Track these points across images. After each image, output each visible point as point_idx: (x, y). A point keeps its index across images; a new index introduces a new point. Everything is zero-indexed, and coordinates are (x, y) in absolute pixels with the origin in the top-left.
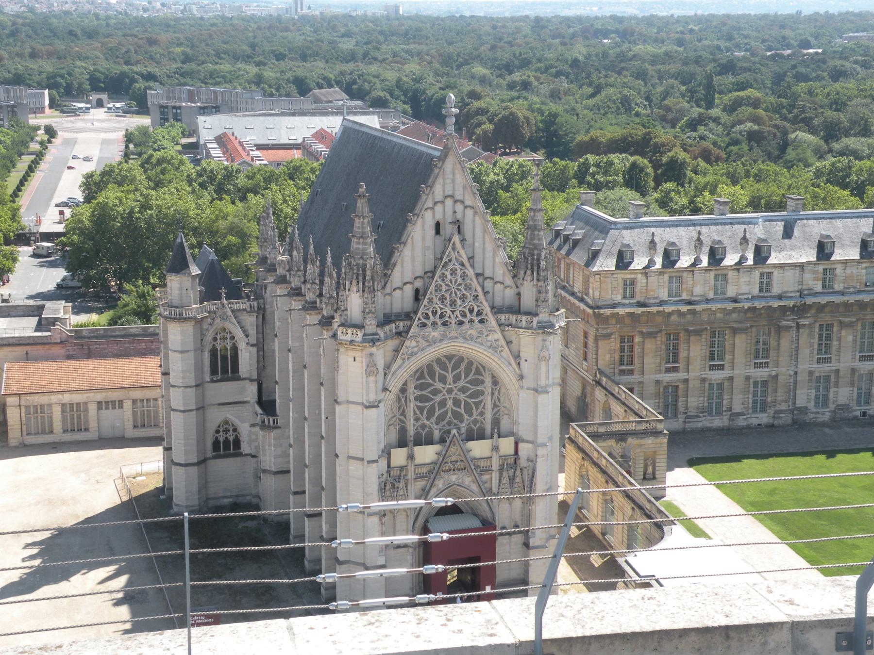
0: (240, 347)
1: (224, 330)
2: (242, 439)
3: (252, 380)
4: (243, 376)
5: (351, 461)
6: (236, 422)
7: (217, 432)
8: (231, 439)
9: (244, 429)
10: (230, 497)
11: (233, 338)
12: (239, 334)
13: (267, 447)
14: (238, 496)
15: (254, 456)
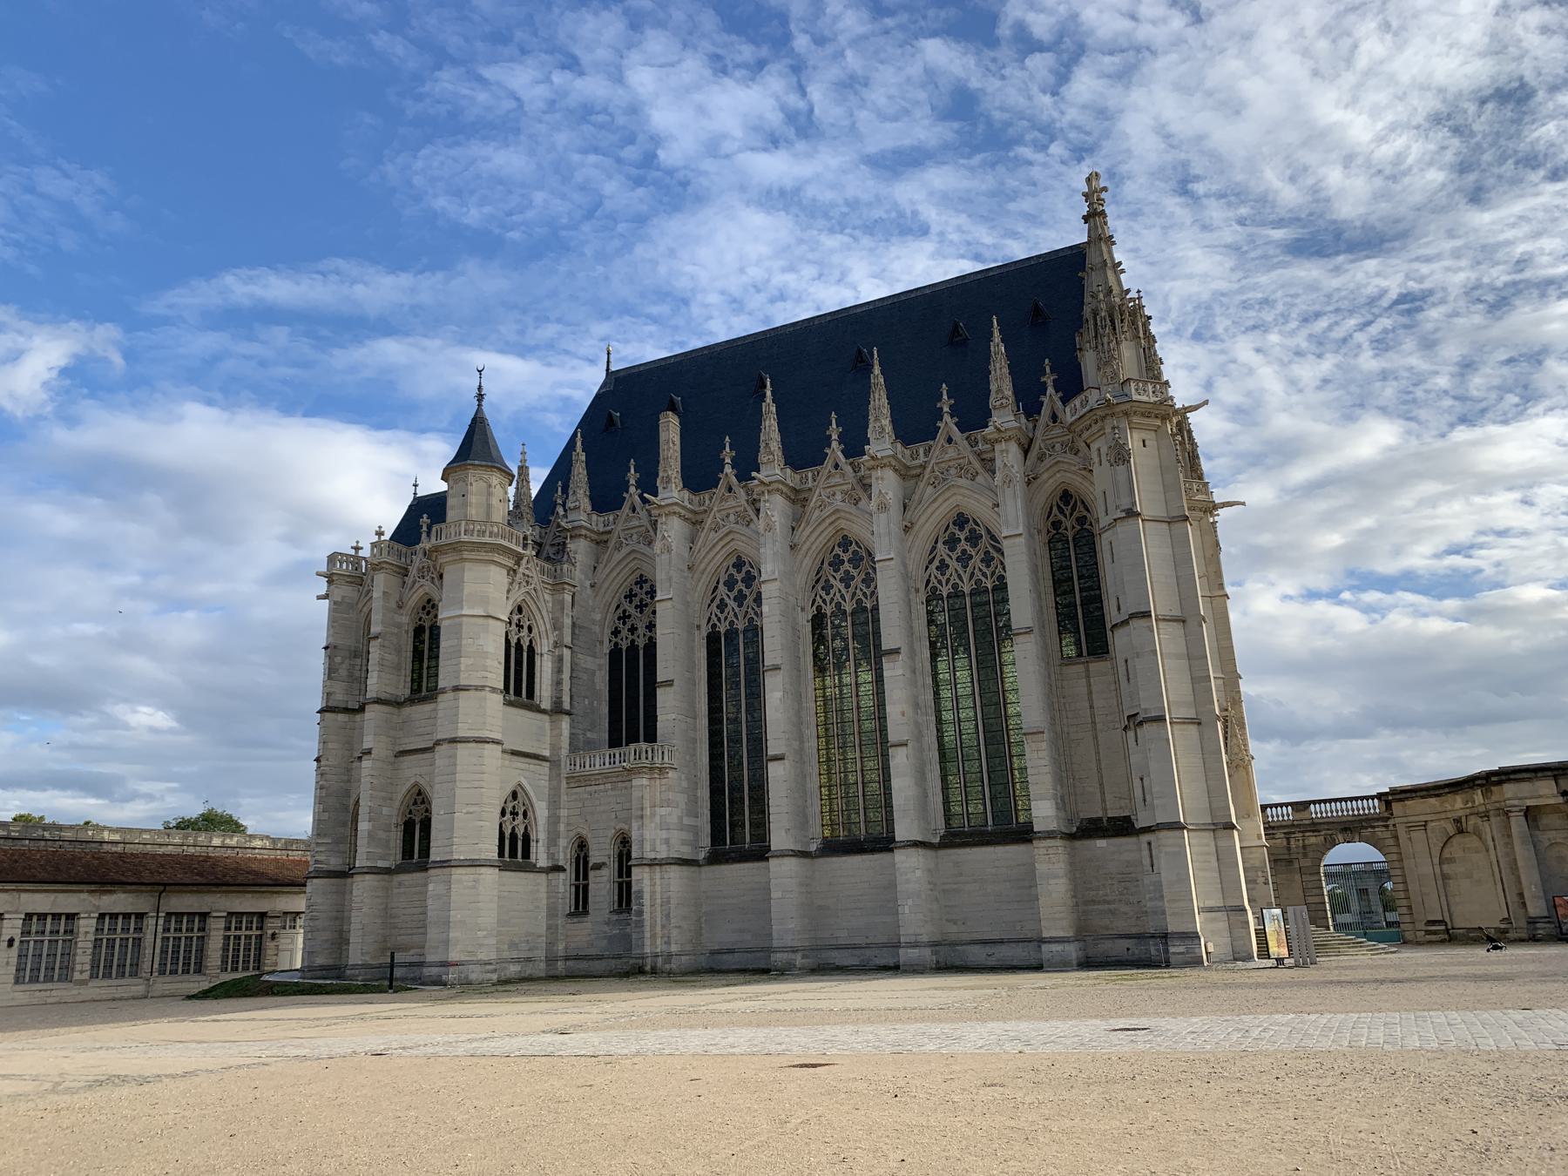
0: (538, 650)
1: (520, 610)
2: (533, 837)
3: (557, 710)
4: (546, 705)
5: (1162, 625)
6: (532, 794)
7: (503, 813)
8: (520, 832)
9: (541, 810)
10: (517, 961)
11: (530, 629)
12: (543, 624)
13: (648, 812)
14: (529, 960)
15: (557, 869)
